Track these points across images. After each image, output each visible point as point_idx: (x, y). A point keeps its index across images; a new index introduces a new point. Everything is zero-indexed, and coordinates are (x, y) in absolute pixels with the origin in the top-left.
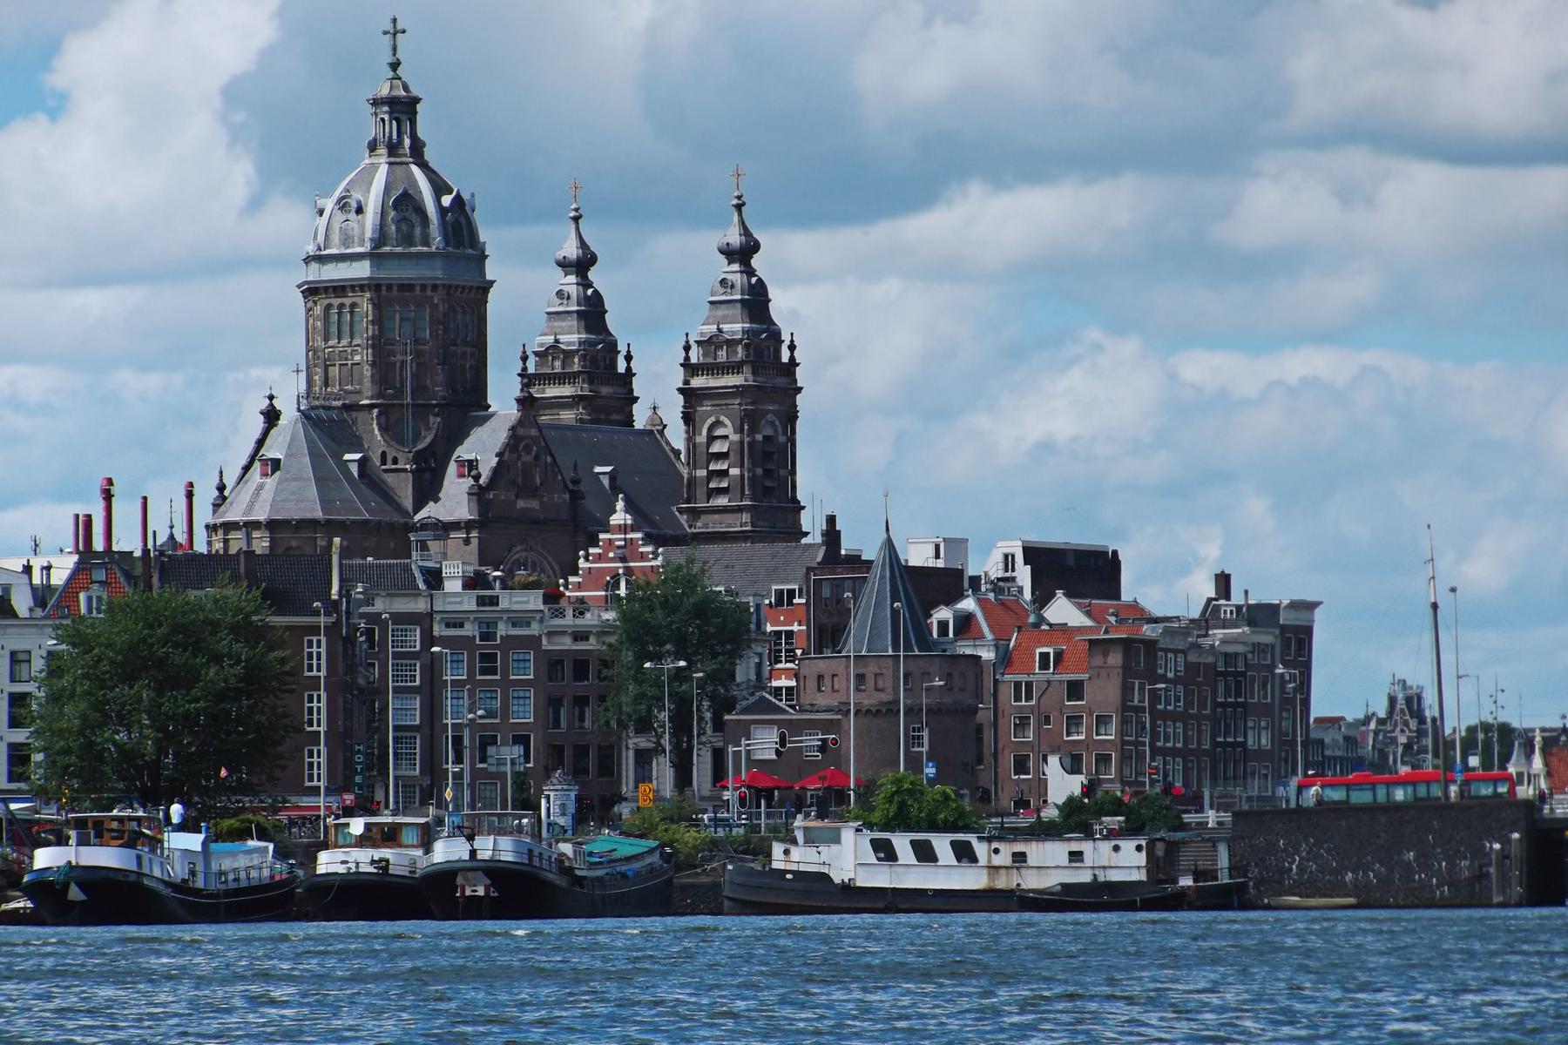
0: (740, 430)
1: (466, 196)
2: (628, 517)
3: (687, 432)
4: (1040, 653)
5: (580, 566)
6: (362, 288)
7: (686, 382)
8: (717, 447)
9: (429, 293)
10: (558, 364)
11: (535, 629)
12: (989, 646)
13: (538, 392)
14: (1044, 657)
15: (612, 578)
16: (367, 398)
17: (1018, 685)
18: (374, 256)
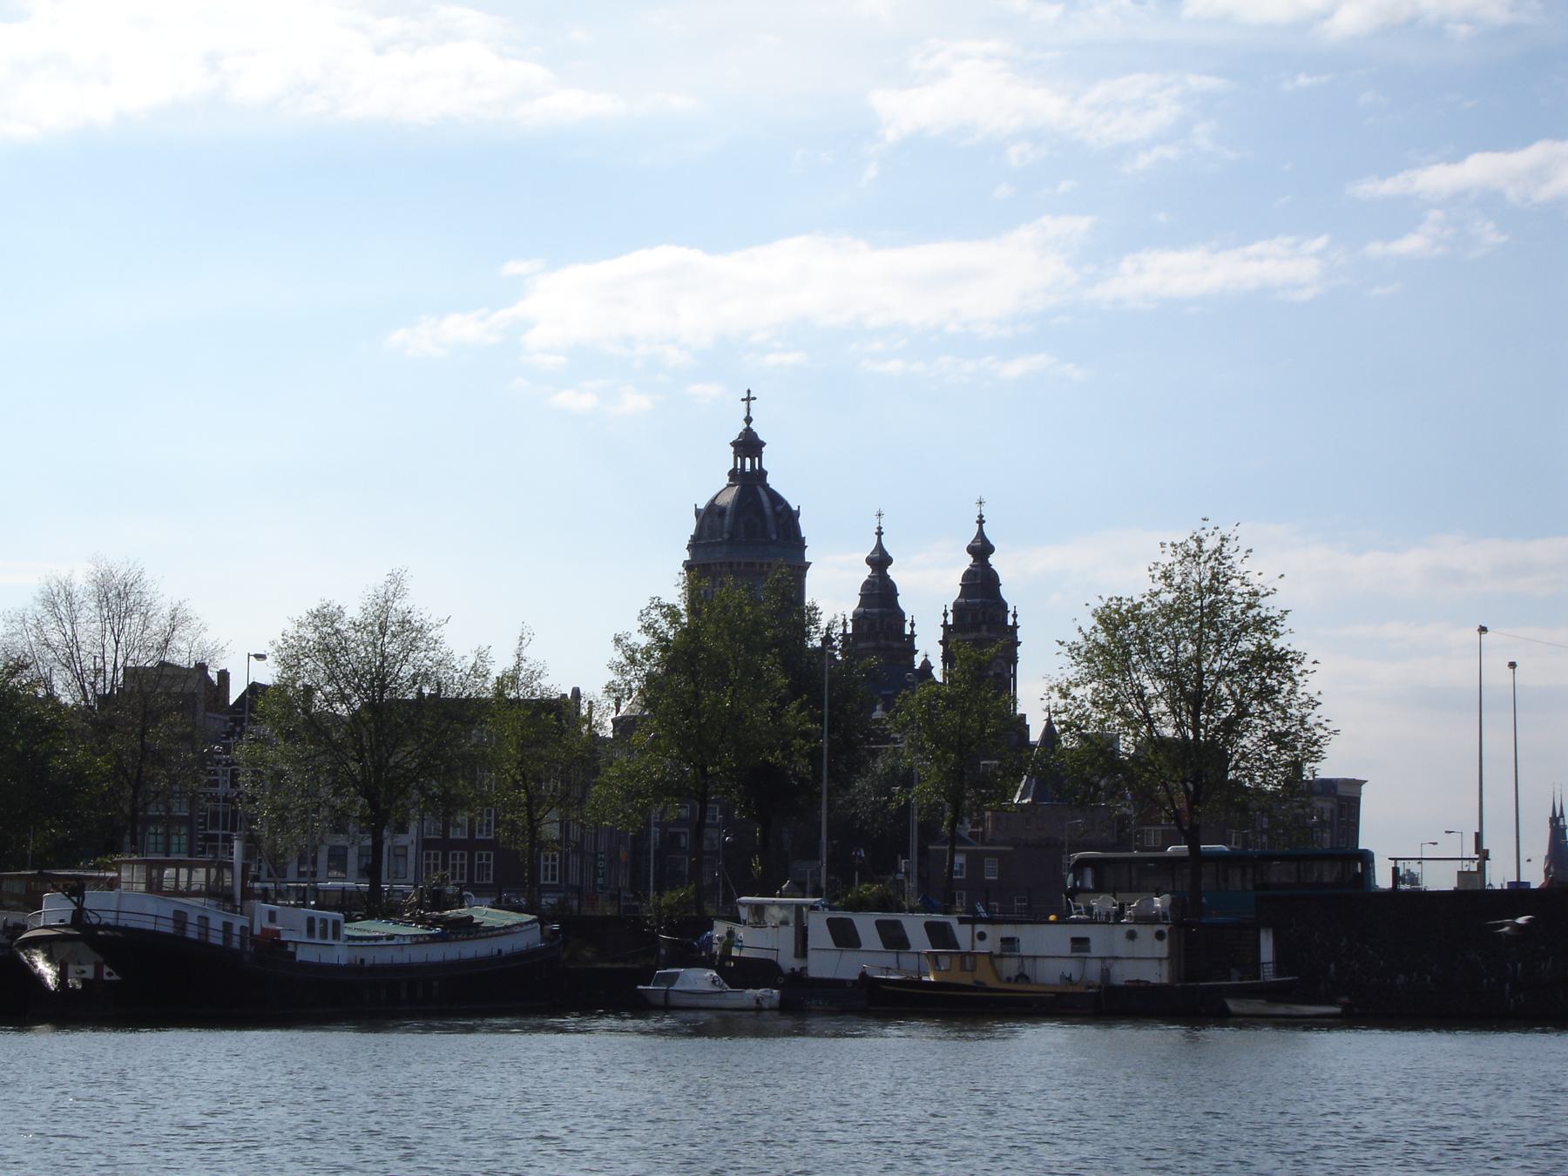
3: (945, 668)
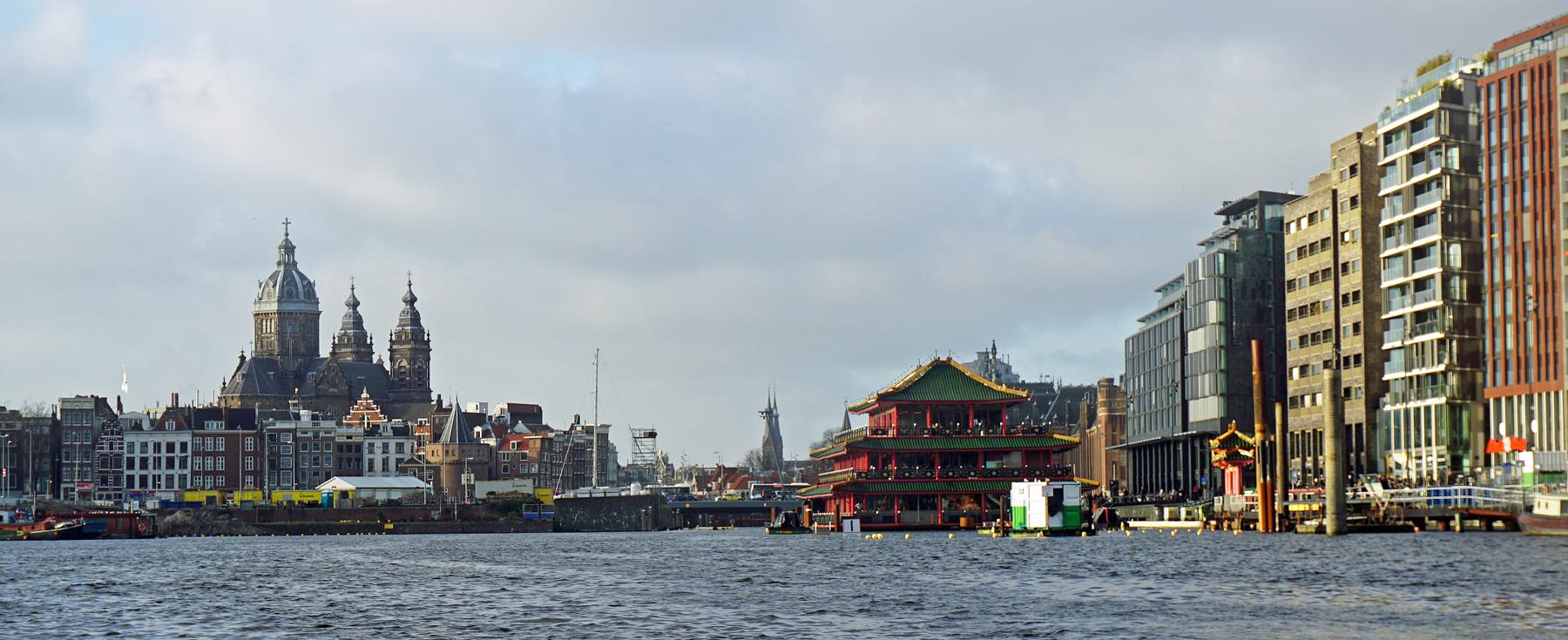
0: (409, 364)
1: (312, 281)
7: (391, 347)
8: (402, 370)
10: (346, 340)
11: (332, 435)
14: (513, 444)
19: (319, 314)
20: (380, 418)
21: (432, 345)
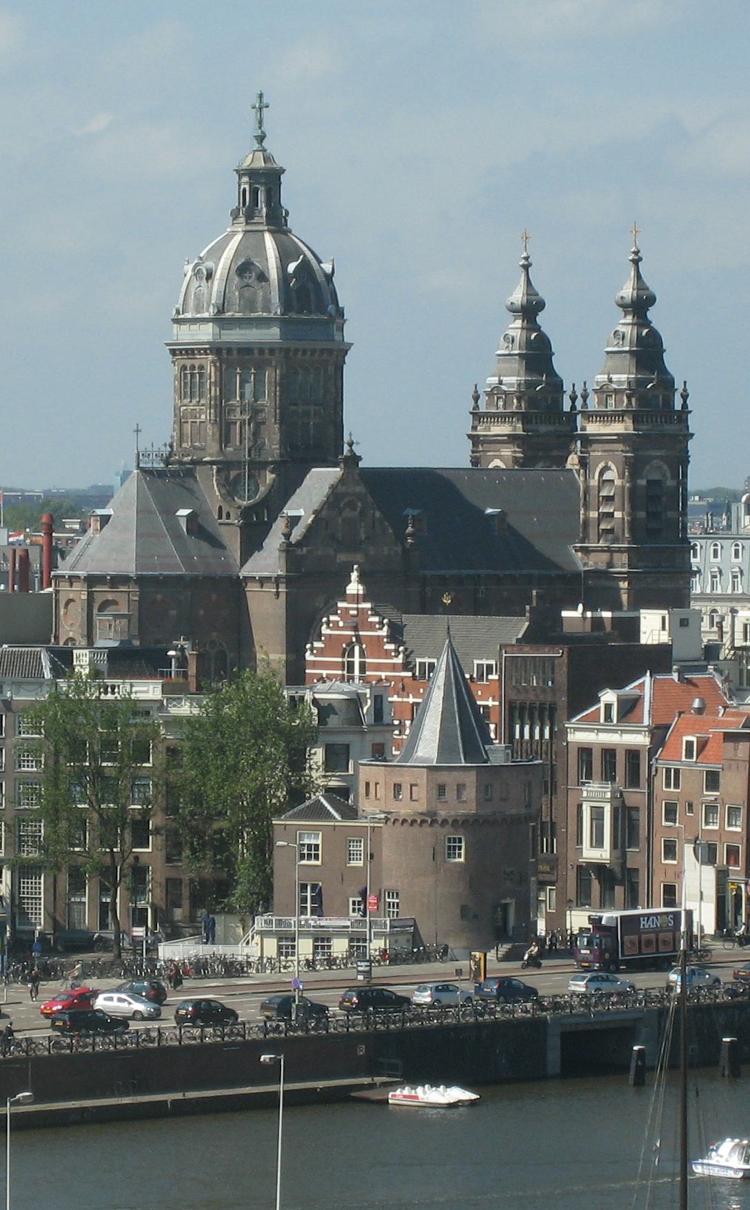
0: (621, 476)
2: (361, 587)
4: (687, 742)
5: (323, 632)
6: (205, 350)
9: (267, 356)
10: (501, 403)
12: (645, 731)
13: (485, 430)
14: (689, 744)
15: (347, 645)
16: (210, 455)
17: (668, 770)
18: (220, 320)
19: (344, 351)
20: (387, 654)
21: (693, 423)
